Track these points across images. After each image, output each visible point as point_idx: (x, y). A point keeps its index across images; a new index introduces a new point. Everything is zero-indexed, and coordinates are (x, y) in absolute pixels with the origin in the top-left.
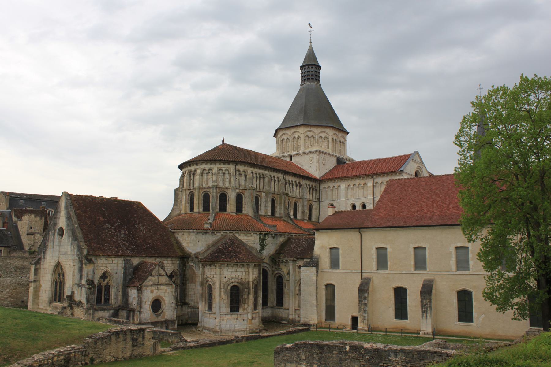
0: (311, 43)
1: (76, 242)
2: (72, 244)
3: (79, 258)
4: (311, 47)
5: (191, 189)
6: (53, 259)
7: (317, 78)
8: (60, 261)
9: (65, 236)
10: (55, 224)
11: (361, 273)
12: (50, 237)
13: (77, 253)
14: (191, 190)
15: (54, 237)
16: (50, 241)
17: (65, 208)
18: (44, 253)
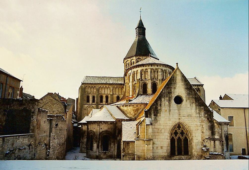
0: (141, 17)
1: (203, 107)
2: (196, 109)
3: (208, 119)
4: (141, 19)
5: (154, 80)
6: (170, 120)
7: (144, 34)
8: (181, 121)
9: (184, 103)
10: (170, 93)
11: (246, 128)
12: (163, 103)
13: (205, 115)
14: (154, 81)
15: (169, 103)
16: (163, 105)
17: (182, 80)
18: (156, 115)
